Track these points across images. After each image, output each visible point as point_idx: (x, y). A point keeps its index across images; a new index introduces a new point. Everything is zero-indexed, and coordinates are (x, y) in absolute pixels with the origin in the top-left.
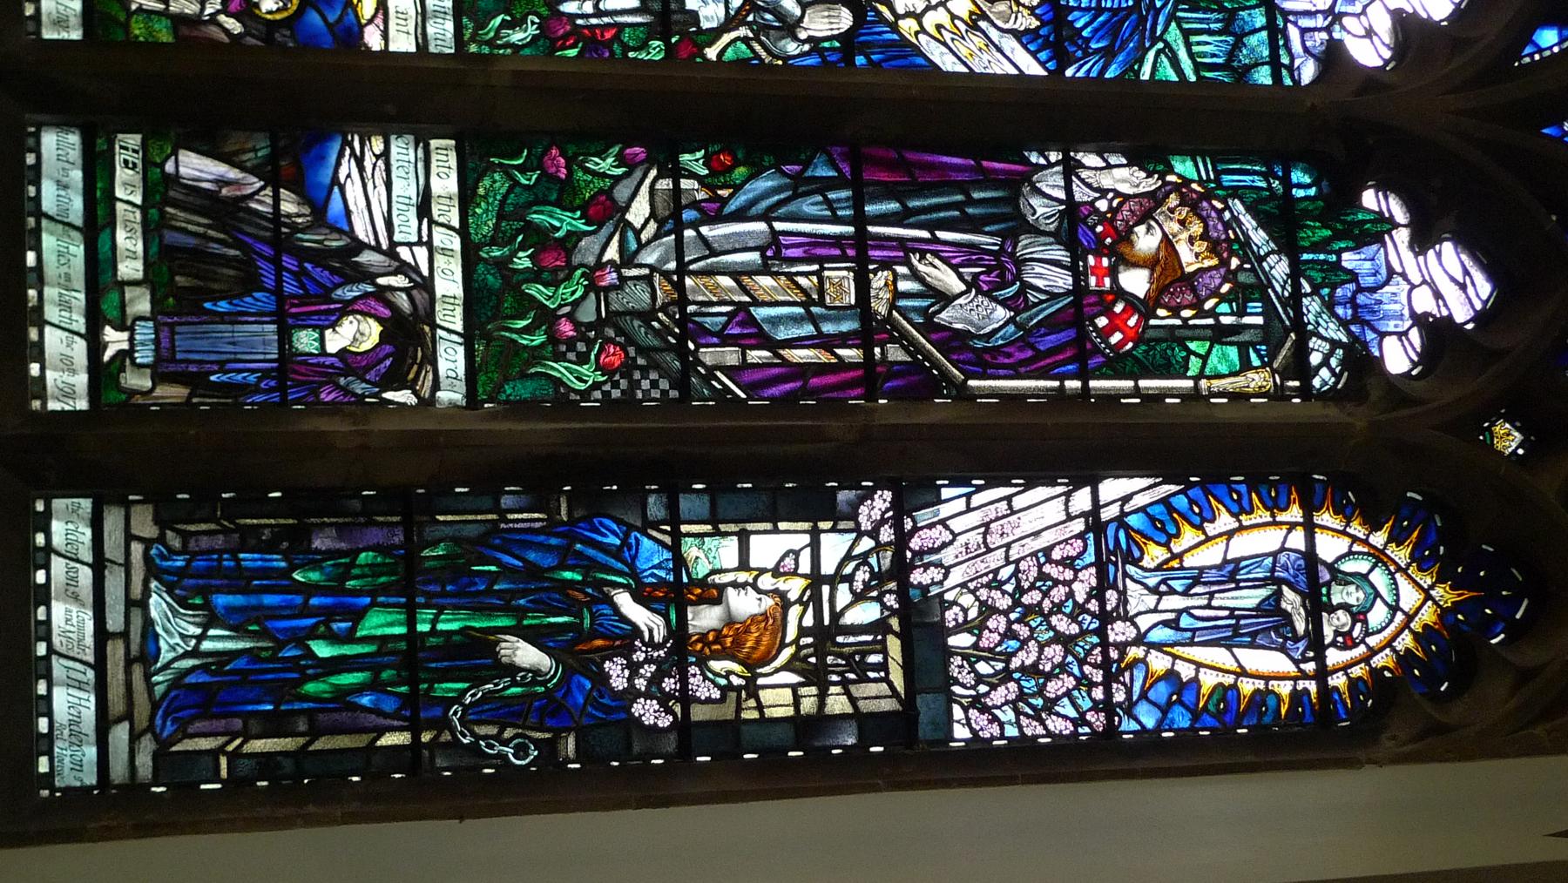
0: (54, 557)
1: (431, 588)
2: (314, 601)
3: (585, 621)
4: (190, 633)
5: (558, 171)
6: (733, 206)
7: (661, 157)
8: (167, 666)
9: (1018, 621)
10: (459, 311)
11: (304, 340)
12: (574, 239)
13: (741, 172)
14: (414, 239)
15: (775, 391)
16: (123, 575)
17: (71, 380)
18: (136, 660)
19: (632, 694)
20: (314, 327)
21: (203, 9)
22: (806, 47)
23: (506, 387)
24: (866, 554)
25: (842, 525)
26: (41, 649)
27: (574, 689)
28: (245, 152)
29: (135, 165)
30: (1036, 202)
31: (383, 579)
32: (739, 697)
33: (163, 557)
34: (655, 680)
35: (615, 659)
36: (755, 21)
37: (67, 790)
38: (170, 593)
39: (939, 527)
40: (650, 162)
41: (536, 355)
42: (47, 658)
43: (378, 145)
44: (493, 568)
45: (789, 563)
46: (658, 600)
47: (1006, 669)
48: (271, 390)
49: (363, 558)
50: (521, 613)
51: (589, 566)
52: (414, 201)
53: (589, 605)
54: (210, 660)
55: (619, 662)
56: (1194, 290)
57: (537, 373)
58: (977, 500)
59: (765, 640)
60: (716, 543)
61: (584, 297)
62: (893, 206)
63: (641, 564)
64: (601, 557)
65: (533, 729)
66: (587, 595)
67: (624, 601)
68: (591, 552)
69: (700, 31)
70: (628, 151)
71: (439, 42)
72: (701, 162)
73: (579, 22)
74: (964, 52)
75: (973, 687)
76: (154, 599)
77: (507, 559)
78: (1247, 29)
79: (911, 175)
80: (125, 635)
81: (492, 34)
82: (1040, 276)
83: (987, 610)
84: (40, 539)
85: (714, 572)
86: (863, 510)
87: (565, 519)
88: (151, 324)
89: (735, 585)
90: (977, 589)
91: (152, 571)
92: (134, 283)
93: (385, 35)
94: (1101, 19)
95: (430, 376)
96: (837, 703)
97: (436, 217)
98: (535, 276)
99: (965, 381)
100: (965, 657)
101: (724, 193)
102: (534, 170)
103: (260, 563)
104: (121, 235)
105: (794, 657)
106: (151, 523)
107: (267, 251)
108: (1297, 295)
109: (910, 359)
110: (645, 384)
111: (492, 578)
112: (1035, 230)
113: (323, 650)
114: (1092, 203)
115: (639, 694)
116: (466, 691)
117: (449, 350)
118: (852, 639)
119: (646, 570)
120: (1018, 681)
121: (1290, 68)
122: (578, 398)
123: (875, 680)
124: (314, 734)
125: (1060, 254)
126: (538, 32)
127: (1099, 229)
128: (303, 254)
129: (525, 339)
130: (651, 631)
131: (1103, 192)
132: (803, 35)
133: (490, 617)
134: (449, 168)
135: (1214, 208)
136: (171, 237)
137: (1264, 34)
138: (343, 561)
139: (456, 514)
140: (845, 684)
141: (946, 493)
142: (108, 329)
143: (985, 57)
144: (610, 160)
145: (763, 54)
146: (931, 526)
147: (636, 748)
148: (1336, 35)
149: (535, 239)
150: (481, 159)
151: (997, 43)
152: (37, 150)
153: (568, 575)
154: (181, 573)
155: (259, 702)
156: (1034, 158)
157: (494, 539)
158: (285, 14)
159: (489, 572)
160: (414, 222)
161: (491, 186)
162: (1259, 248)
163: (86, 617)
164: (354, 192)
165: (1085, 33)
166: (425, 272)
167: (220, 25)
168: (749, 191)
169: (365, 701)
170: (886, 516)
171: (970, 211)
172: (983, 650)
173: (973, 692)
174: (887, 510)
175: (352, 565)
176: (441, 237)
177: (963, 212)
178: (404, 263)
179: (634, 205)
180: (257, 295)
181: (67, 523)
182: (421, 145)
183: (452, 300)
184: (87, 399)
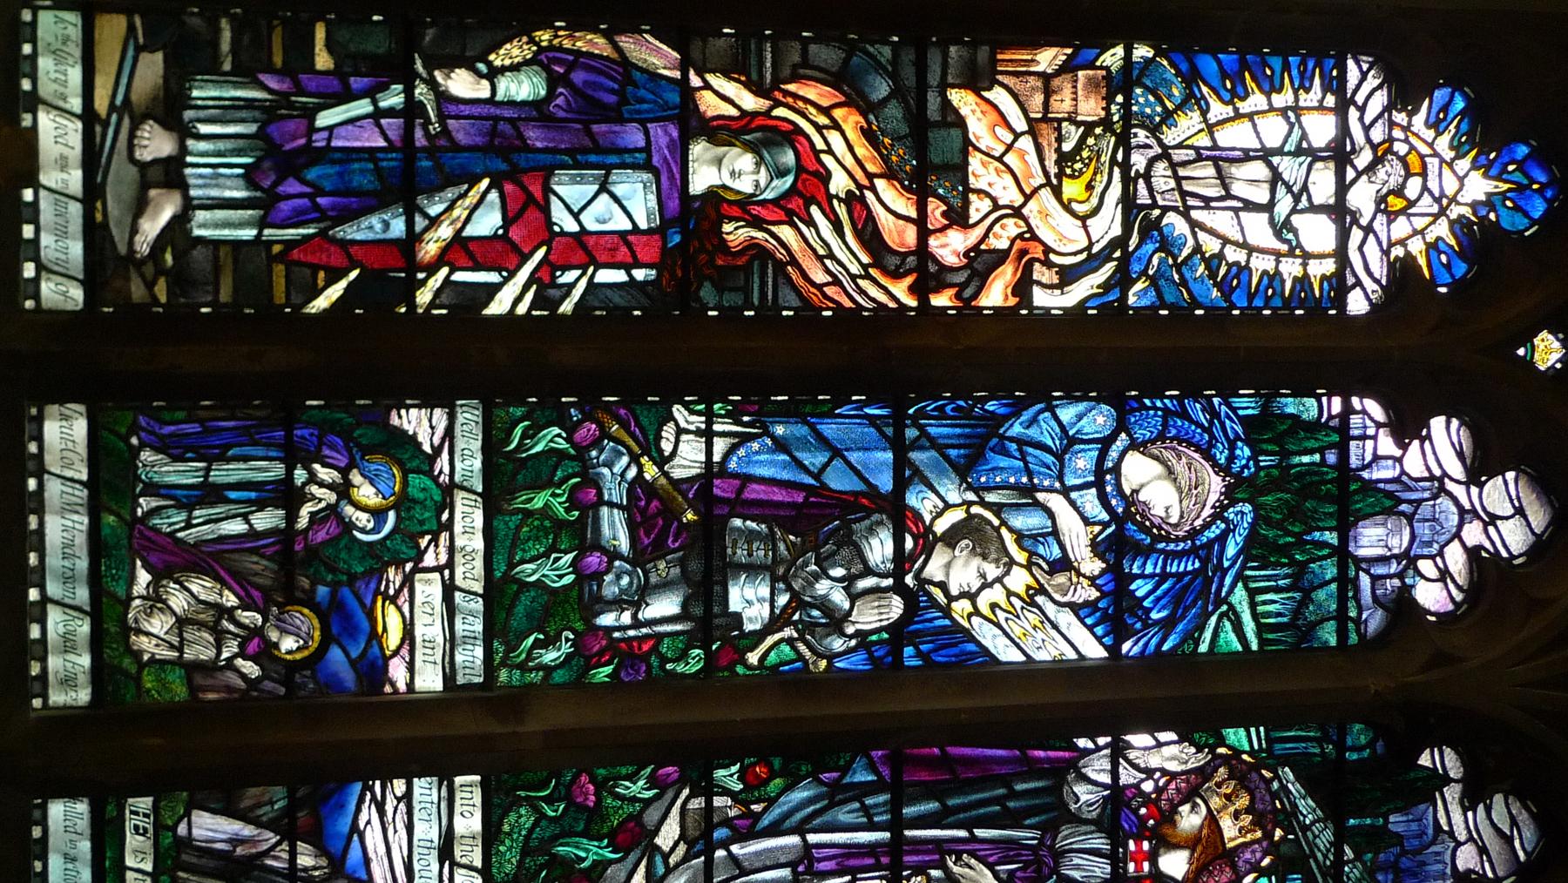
5: (587, 799)
6: (766, 821)
7: (694, 775)
12: (600, 868)
13: (778, 782)
21: (219, 653)
22: (853, 642)
28: (259, 805)
29: (145, 830)
30: (1081, 790)
36: (801, 620)
40: (681, 783)
43: (399, 786)
56: (1234, 867)
62: (933, 806)
69: (743, 635)
70: (660, 772)
71: (468, 671)
72: (736, 776)
73: (616, 635)
74: (1016, 630)
78: (1317, 582)
79: (952, 772)
81: (524, 656)
82: (1078, 867)
94: (1165, 586)
97: (458, 859)
101: (756, 808)
102: (560, 800)
108: (1339, 861)
112: (1076, 819)
114: (1137, 786)
121: (1357, 621)
125: (1100, 842)
127: (1143, 811)
131: (1149, 772)
132: (850, 630)
135: (1262, 776)
137: (1334, 586)
143: (1040, 635)
144: (641, 783)
145: (807, 653)
148: (1409, 581)
151: (1053, 618)
156: (1083, 743)
158: (306, 653)
160: (435, 867)
162: (1305, 816)
164: (374, 838)
165: (1146, 604)
168: (784, 804)
171: (1011, 804)
177: (1004, 807)
179: (665, 828)
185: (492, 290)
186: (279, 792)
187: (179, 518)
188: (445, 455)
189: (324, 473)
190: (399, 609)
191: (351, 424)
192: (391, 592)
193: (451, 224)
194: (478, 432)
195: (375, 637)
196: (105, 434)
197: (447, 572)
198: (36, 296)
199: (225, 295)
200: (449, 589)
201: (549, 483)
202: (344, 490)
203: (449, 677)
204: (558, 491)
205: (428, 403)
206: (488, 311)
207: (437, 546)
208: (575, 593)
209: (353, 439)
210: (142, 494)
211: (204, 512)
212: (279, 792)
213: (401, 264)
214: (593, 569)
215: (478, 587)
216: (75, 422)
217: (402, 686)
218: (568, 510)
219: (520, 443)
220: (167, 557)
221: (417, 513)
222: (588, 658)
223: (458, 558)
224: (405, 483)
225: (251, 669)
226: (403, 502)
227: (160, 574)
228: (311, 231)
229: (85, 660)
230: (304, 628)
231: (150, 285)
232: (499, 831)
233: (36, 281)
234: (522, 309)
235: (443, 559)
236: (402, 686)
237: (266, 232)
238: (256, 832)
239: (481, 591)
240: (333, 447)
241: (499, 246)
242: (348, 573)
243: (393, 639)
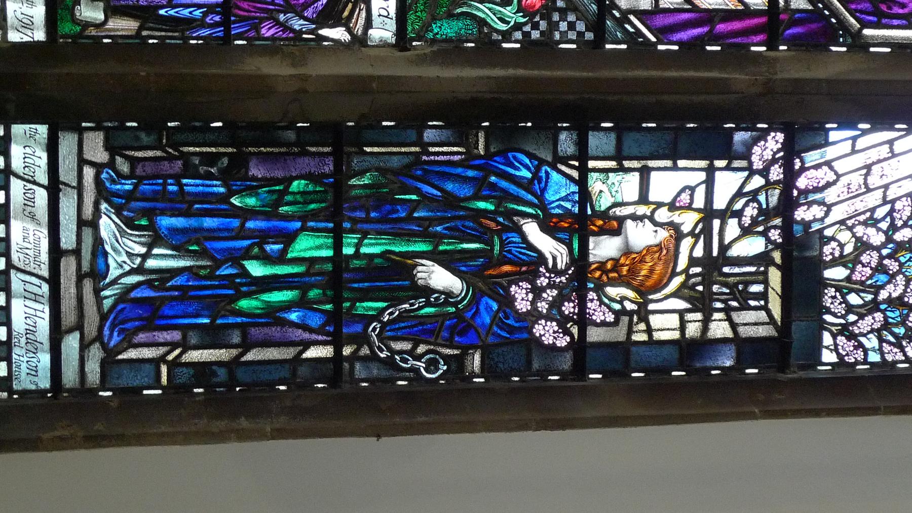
2: (250, 224)
3: (496, 247)
4: (136, 252)
8: (114, 282)
9: (889, 256)
15: (684, 35)
16: (76, 197)
18: (87, 275)
19: (534, 315)
23: (434, 26)
24: (756, 192)
25: (737, 164)
27: (482, 307)
31: (313, 206)
32: (631, 321)
33: (113, 182)
34: (556, 304)
35: (521, 284)
37: (24, 393)
38: (118, 214)
39: (825, 168)
44: (414, 197)
45: (685, 198)
46: (563, 230)
47: (874, 300)
48: (216, 25)
49: (297, 186)
50: (437, 239)
53: (499, 233)
54: (154, 277)
55: (524, 286)
57: (463, 13)
58: (861, 143)
59: (659, 269)
60: (619, 178)
63: (550, 196)
64: (513, 189)
65: (443, 346)
66: (498, 223)
67: (532, 230)
68: (504, 184)
75: (843, 317)
76: (104, 222)
80: (77, 252)
83: (862, 246)
85: (616, 205)
86: (756, 150)
87: (482, 153)
89: (634, 217)
90: (854, 226)
91: (102, 193)
95: (363, 14)
96: (720, 329)
99: (860, 30)
100: (838, 289)
103: (201, 188)
105: (684, 285)
106: (102, 149)
109: (811, 8)
110: (563, 26)
111: (415, 205)
113: (256, 269)
115: (540, 316)
116: (384, 310)
118: (737, 270)
119: (553, 202)
120: (883, 311)
123: (756, 308)
124: (246, 346)
130: (554, 258)
138: (277, 188)
140: (727, 310)
141: (833, 136)
146: (817, 167)
147: (536, 365)
153: (482, 205)
154: (129, 196)
155: (197, 316)
157: (416, 170)
159: (410, 201)
163: (41, 235)
169: (294, 316)
170: (777, 156)
172: (856, 283)
173: (842, 321)
174: (779, 151)
175: (286, 192)
181: (24, 147)
184: (44, 30)
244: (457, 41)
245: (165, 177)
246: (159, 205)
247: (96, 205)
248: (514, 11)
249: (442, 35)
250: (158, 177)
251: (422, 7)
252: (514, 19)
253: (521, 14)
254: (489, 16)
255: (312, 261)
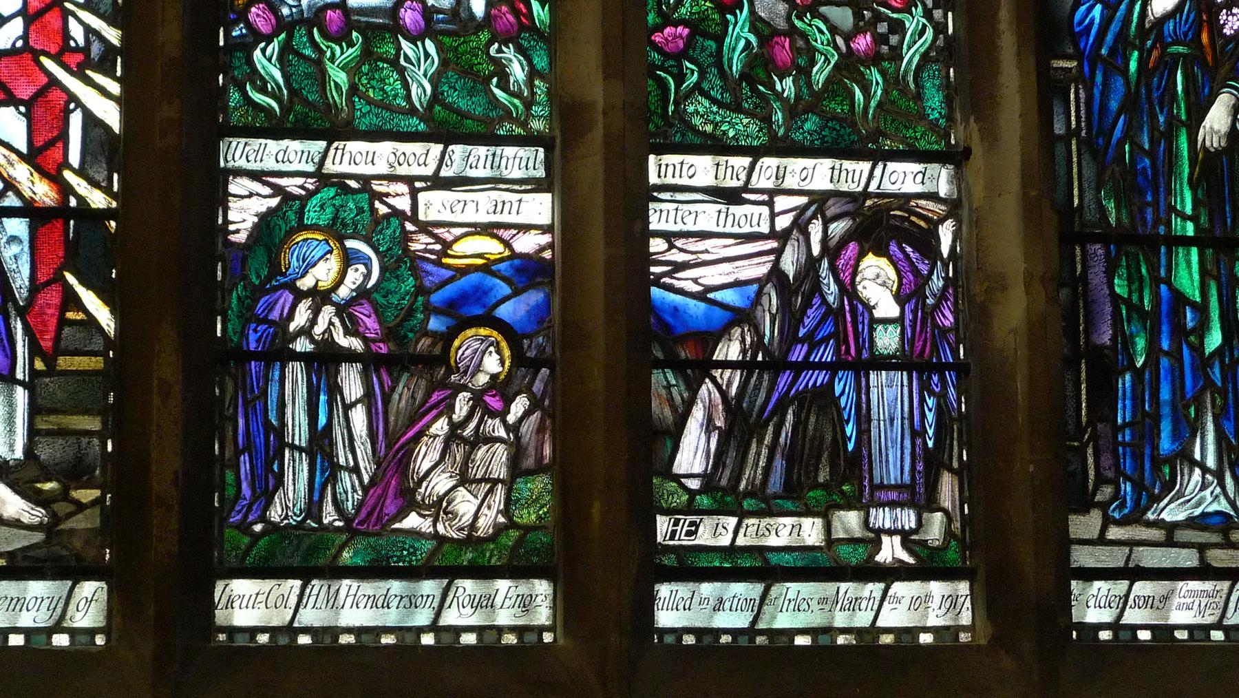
0: (1124, 621)
1: (1149, 217)
2: (1165, 345)
3: (1181, 51)
4: (1200, 479)
10: (847, 164)
11: (887, 341)
12: (759, 25)
14: (765, 210)
16: (1141, 549)
17: (937, 600)
20: (872, 330)
21: (500, 440)
23: (931, 117)
26: (1217, 635)
28: (671, 399)
29: (692, 524)
31: (1144, 271)
33: (1122, 505)
35: (1222, 22)
38: (1159, 499)
41: (893, 82)
42: (1227, 630)
43: (657, 245)
49: (1120, 288)
50: (1173, 121)
51: (1123, 44)
52: (723, 207)
53: (1165, 46)
54: (1225, 459)
55: (1225, 17)
61: (825, 20)
64: (1114, 27)
66: (1153, 47)
68: (1109, 38)
71: (531, 165)
76: (1167, 516)
77: (1117, 133)
80: (1202, 548)
81: (516, 101)
84: (1105, 635)
88: (873, 511)
91: (1135, 518)
92: (828, 528)
93: (525, 228)
95: (922, 202)
97: (740, 184)
98: (804, 73)
102: (680, 66)
103: (1128, 402)
104: (773, 541)
106: (1087, 517)
107: (784, 379)
117: (893, 179)
122: (941, 36)
126: (511, 45)
128: (789, 337)
129: (875, 92)
133: (1178, 156)
134: (682, 163)
136: (776, 482)
138: (1124, 312)
139: (1072, 185)
142: (880, 558)
149: (761, 74)
150: (671, 125)
152: (679, 632)
153: (1133, 66)
154: (1138, 487)
158: (504, 344)
159: (1130, 152)
160: (747, 209)
161: (702, 116)
163: (1185, 589)
164: (712, 276)
166: (803, 200)
167: (520, 420)
175: (1128, 302)
176: (764, 179)
178: (795, 223)
180: (838, 390)
181: (1088, 607)
182: (655, 194)
183: (837, 172)
184: (957, 583)
185: (91, 122)
186: (657, 378)
187: (346, 479)
188: (283, 182)
189: (301, 317)
190: (457, 239)
191: (245, 287)
192: (438, 247)
193: (12, 165)
194: (256, 143)
195: (488, 268)
196: (249, 560)
197: (418, 185)
198: (92, 632)
199: (93, 424)
200: (438, 182)
201: (319, 63)
202: (320, 297)
203: (538, 186)
204: (328, 54)
205: (222, 199)
206: (116, 126)
207: (387, 195)
208: (447, 40)
209: (263, 284)
210: (319, 520)
211: (341, 453)
212: (657, 378)
213: (59, 224)
214: (420, 18)
215: (436, 149)
216: (235, 593)
217: (546, 239)
218: (351, 44)
219: (272, 95)
220: (391, 492)
221: (349, 215)
222: (522, 28)
223: (403, 171)
224: (315, 228)
225: (519, 406)
226: (336, 231)
227: (410, 502)
228: (19, 326)
229: (503, 585)
230: (476, 345)
231: (80, 507)
232: (711, 136)
233: (73, 632)
234: (115, 88)
235: (402, 188)
236: (546, 239)
237: (19, 376)
238: (700, 405)
239: (440, 147)
240: (270, 307)
241: (39, 112)
242: (416, 294)
243: (492, 247)
244: (946, 86)
245: (1116, 444)
246: (1147, 451)
247: (1150, 524)
248: (911, 18)
249: (942, 108)
250: (1116, 452)
251: (911, 131)
252: (920, 19)
253: (913, 9)
254: (918, 48)
255: (1203, 272)
